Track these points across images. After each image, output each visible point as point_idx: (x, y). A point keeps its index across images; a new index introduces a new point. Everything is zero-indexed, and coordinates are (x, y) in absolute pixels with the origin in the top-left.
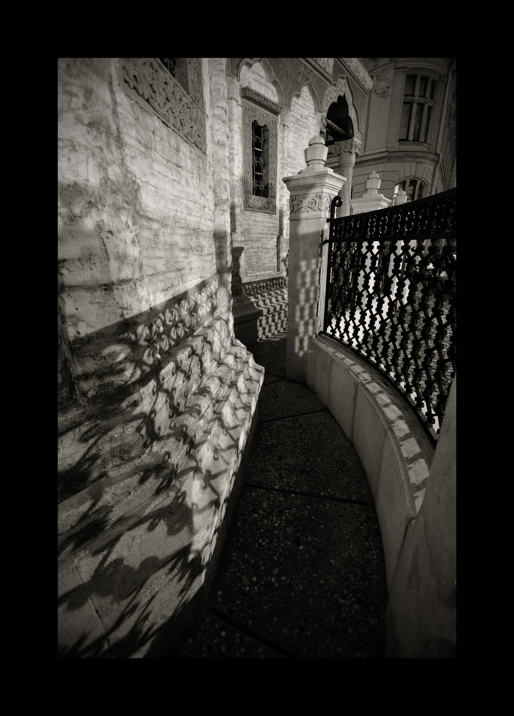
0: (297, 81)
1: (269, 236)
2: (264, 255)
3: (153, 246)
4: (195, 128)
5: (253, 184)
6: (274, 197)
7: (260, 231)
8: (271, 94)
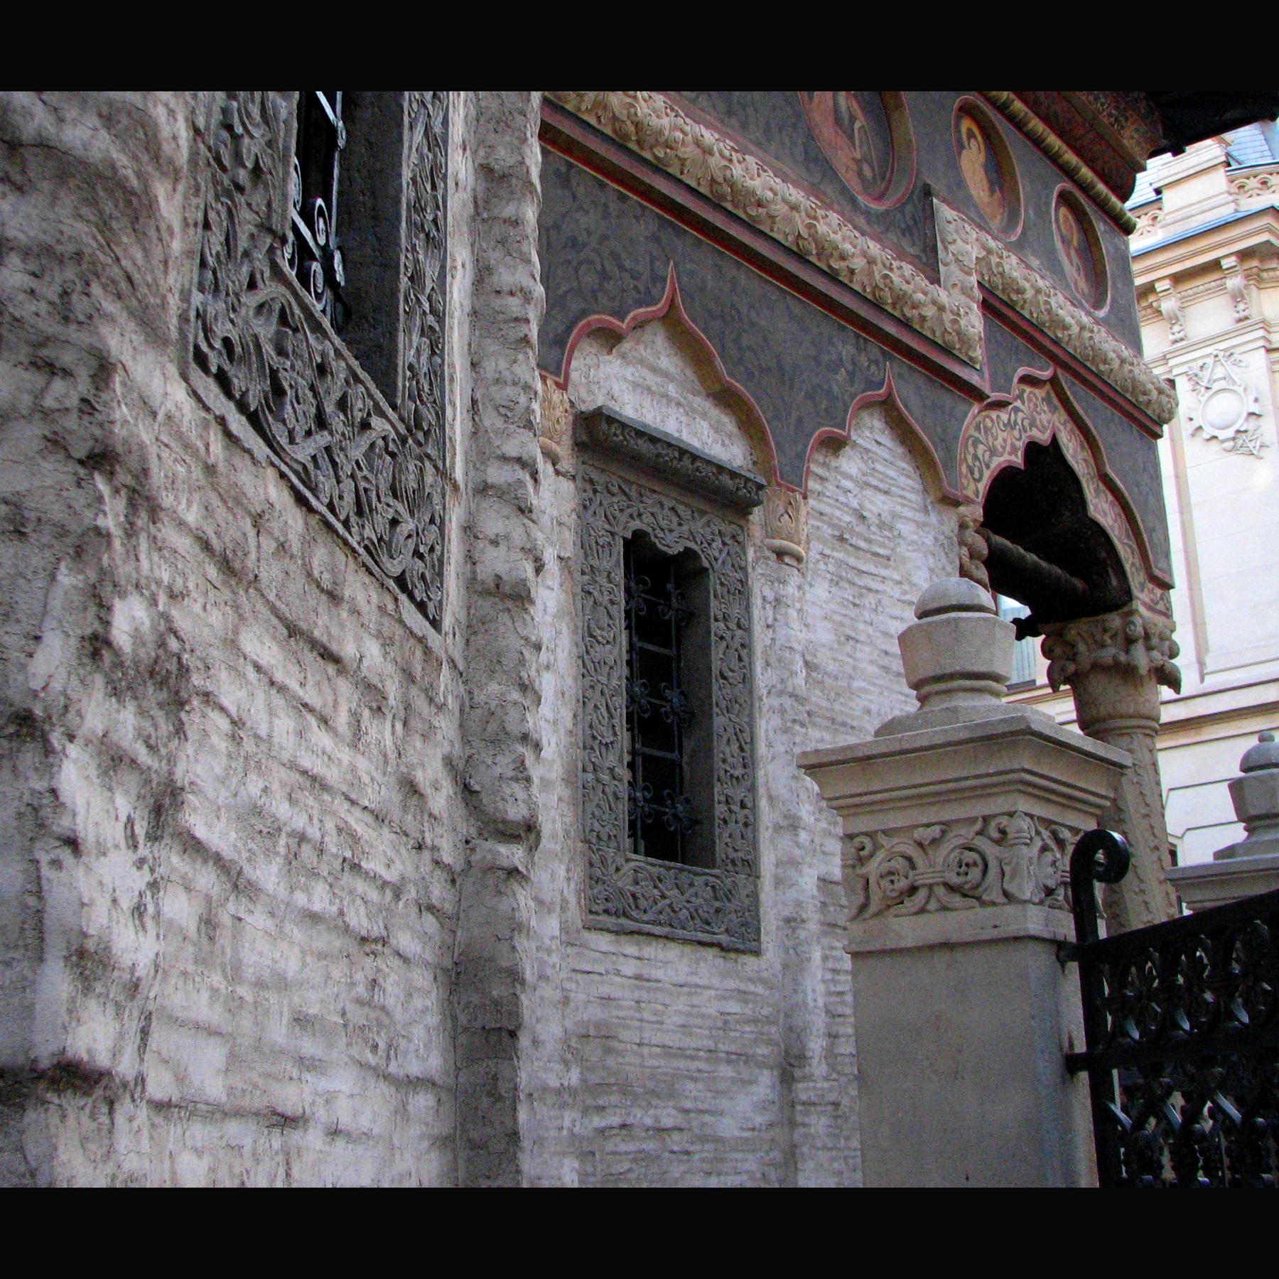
0: (828, 393)
1: (726, 1071)
3: (191, 968)
4: (408, 525)
5: (632, 799)
6: (750, 866)
7: (674, 1040)
8: (711, 437)
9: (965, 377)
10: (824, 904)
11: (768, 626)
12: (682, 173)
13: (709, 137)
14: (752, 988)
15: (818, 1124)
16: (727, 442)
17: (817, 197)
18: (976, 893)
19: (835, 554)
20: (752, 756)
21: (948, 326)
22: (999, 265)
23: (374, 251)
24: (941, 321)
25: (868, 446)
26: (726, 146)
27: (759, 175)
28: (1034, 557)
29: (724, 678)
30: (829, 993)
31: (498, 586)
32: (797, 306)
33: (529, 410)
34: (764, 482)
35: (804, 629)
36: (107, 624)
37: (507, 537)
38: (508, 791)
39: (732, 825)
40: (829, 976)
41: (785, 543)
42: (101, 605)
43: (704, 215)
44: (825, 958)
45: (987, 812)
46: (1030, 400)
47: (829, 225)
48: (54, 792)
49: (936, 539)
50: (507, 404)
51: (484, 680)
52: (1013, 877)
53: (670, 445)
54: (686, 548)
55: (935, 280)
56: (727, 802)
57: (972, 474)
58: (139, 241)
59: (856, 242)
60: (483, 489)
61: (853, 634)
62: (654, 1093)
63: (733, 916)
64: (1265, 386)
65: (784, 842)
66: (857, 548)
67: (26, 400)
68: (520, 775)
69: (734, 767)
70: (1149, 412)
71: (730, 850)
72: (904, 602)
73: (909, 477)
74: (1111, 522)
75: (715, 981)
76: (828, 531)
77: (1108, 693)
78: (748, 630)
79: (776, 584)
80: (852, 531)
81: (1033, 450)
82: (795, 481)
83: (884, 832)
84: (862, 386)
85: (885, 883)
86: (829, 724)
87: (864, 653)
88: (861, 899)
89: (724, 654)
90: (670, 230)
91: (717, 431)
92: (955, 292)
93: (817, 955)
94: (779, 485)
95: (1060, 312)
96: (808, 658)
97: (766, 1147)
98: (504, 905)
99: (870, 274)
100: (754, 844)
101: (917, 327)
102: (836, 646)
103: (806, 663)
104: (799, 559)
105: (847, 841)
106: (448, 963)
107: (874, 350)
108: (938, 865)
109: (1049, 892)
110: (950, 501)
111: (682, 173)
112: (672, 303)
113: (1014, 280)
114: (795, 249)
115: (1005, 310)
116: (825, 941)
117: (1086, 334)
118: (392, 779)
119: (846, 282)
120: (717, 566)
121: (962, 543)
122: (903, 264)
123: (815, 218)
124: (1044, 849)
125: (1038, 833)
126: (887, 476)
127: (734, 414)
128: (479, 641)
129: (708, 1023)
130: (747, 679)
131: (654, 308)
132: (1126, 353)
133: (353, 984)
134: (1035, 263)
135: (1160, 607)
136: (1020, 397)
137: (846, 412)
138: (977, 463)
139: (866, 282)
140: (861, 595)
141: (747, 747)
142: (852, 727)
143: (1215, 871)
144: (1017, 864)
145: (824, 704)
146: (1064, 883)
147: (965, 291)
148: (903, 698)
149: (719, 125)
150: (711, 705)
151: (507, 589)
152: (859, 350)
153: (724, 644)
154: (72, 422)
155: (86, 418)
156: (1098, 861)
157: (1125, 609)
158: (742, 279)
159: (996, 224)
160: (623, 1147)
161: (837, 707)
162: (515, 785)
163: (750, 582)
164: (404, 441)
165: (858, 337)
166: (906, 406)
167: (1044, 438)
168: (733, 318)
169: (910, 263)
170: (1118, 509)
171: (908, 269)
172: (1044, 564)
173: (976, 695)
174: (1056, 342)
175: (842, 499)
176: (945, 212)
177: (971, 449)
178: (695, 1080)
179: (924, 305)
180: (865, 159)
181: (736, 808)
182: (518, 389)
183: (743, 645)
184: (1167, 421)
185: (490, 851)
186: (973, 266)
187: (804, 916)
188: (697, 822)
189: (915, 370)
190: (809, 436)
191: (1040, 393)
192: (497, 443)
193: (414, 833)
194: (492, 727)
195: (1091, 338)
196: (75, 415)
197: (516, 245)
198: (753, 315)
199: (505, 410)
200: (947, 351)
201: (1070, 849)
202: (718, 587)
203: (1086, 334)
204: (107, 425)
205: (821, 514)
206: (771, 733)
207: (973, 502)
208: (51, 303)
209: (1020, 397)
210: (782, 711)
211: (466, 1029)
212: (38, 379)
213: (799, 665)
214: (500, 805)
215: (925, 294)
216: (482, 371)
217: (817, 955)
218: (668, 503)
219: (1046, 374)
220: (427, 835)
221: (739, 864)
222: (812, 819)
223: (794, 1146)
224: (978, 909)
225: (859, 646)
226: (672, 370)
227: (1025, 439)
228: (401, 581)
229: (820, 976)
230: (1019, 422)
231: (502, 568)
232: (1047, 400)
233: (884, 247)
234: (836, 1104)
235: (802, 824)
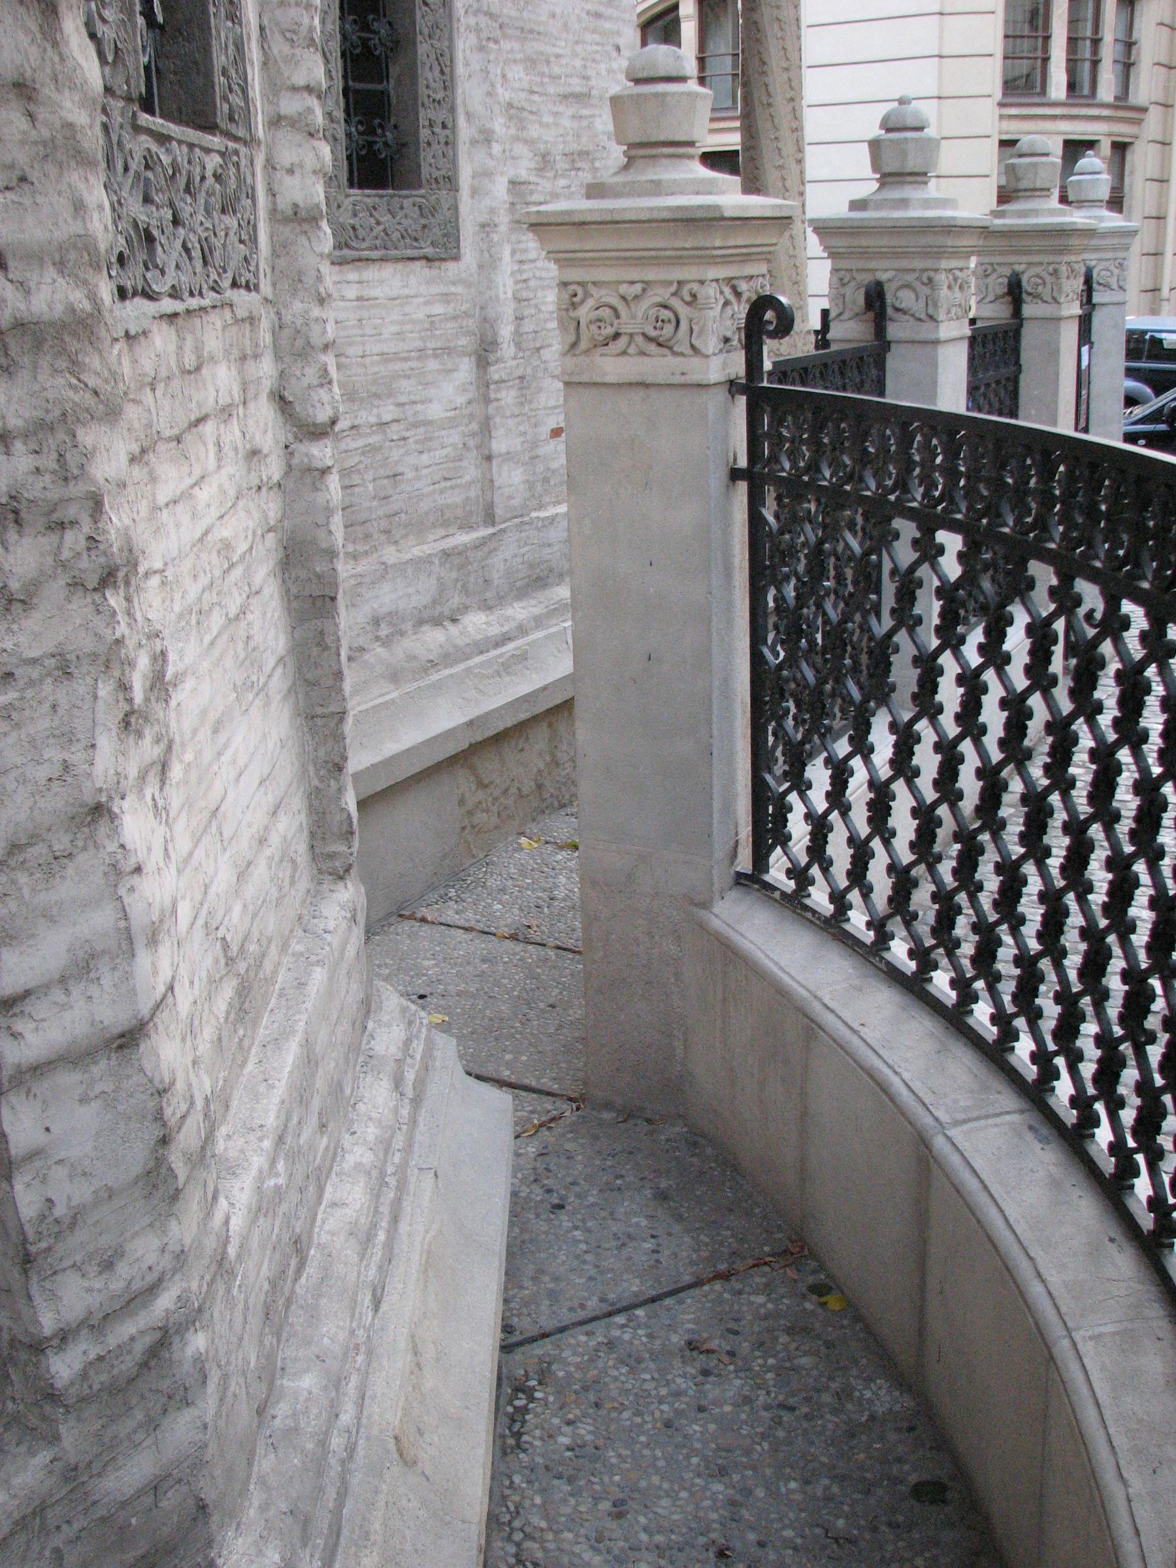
1: (433, 365)
2: (412, 460)
5: (349, 135)
6: (450, 181)
7: (389, 348)
10: (513, 204)
14: (453, 289)
15: (508, 397)
30: (516, 282)
33: (311, 29)
37: (301, 166)
38: (316, 398)
39: (435, 146)
44: (513, 252)
45: (681, 278)
48: (122, 846)
62: (376, 396)
63: (436, 230)
65: (480, 155)
67: (49, 560)
69: (435, 92)
75: (423, 289)
83: (594, 283)
85: (593, 327)
86: (518, 33)
88: (572, 338)
97: (466, 421)
98: (320, 498)
100: (454, 163)
108: (636, 319)
116: (513, 237)
128: (282, 263)
141: (447, 70)
151: (303, 214)
154: (84, 563)
155: (93, 553)
160: (353, 445)
161: (525, 14)
173: (676, 161)
178: (408, 377)
181: (438, 130)
188: (404, 145)
196: (85, 556)
208: (54, 472)
210: (478, 30)
211: (296, 597)
212: (54, 538)
214: (310, 410)
223: (488, 419)
234: (522, 378)
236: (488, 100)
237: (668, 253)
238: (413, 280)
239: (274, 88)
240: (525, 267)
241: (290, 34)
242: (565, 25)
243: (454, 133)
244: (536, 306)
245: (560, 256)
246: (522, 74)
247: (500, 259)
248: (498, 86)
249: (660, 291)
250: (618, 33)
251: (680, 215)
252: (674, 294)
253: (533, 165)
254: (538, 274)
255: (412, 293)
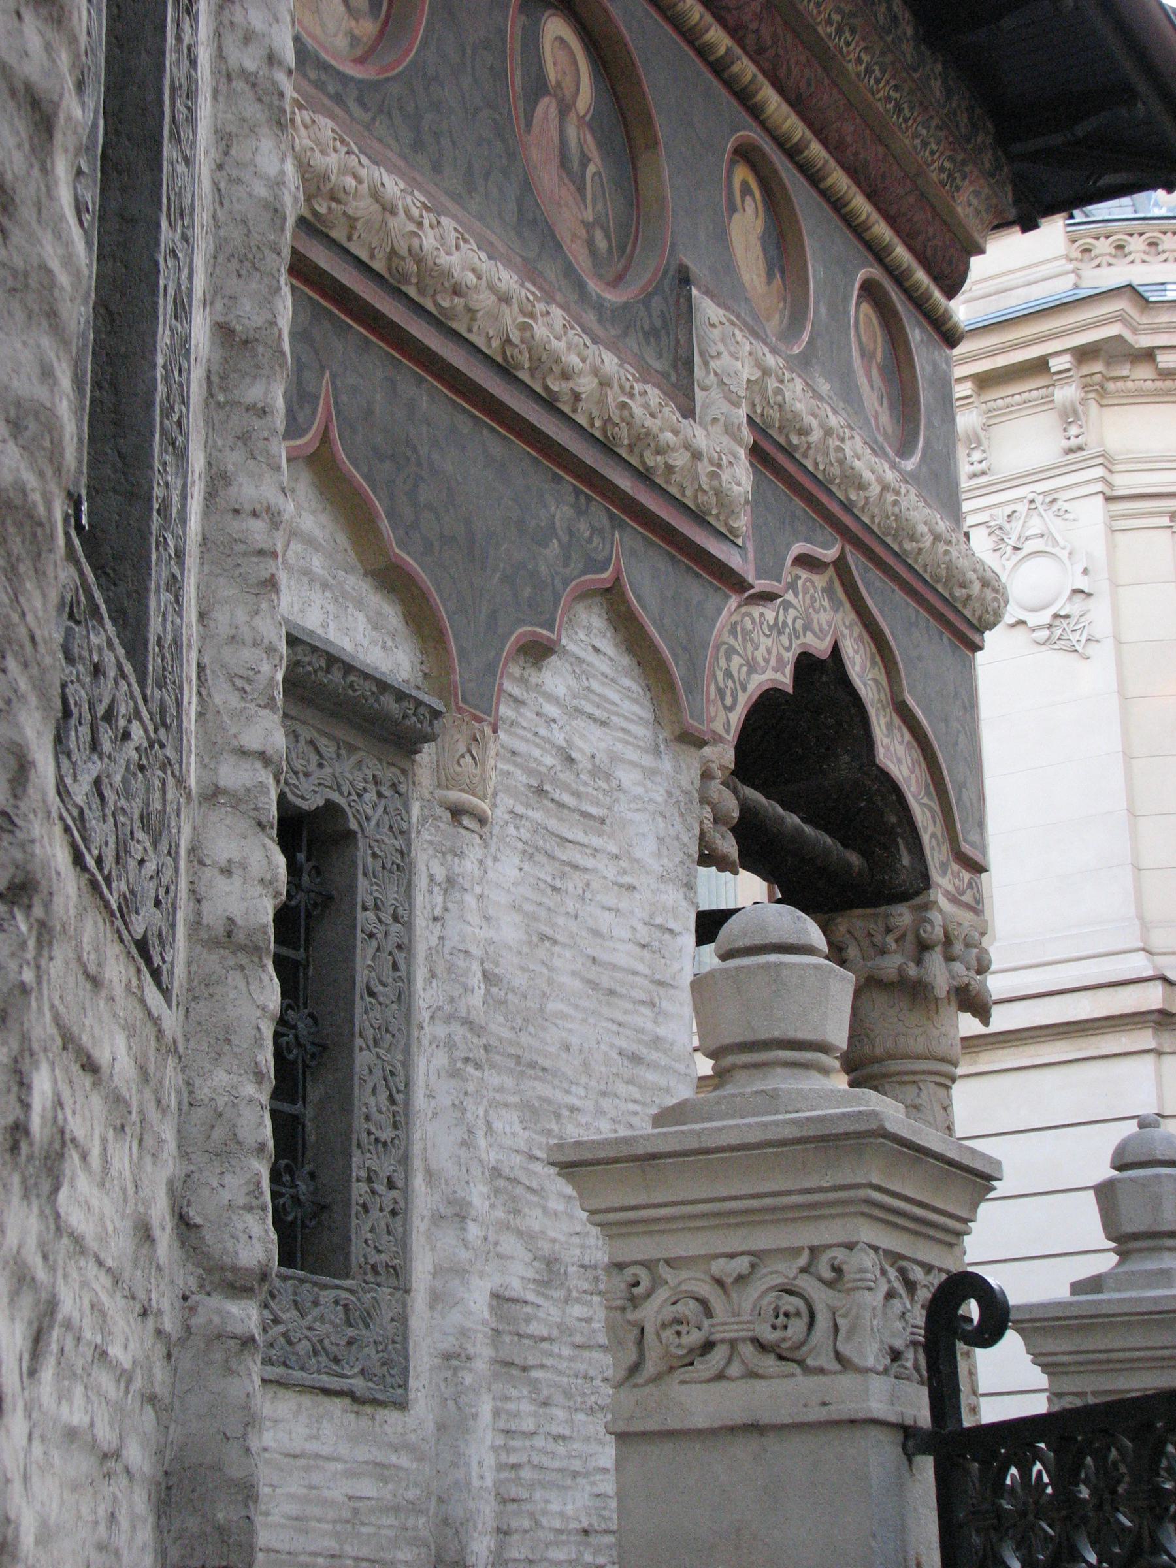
4: (151, 867)
6: (397, 1273)
8: (372, 639)
9: (721, 557)
11: (435, 919)
12: (350, 239)
13: (393, 186)
14: (394, 1459)
16: (390, 643)
17: (534, 284)
18: (797, 1355)
19: (530, 813)
20: (406, 1115)
21: (704, 481)
22: (778, 391)
23: (115, 472)
24: (696, 477)
25: (582, 654)
26: (414, 201)
27: (458, 248)
28: (797, 819)
29: (372, 994)
30: (501, 1467)
31: (229, 934)
32: (496, 445)
34: (443, 709)
35: (484, 924)
36: (26, 1106)
37: (243, 866)
39: (375, 1213)
40: (500, 1441)
41: (465, 797)
42: (21, 1084)
43: (378, 306)
44: (496, 1413)
45: (816, 1242)
46: (805, 593)
47: (550, 326)
49: (669, 794)
50: (245, 673)
51: (208, 1067)
52: (849, 1338)
53: (315, 649)
54: (327, 801)
55: (688, 412)
56: (369, 1180)
57: (722, 698)
58: (40, 587)
59: (588, 352)
60: (213, 795)
61: (548, 931)
63: (371, 1350)
64: (1099, 549)
65: (447, 1239)
66: (561, 805)
68: (255, 1203)
70: (967, 613)
71: (370, 1251)
72: (621, 886)
73: (636, 701)
74: (906, 772)
75: (344, 1450)
76: (521, 778)
77: (894, 1025)
78: (408, 925)
79: (449, 857)
80: (554, 781)
81: (806, 665)
82: (482, 708)
83: (668, 1262)
84: (581, 566)
85: (668, 1334)
86: (511, 1064)
87: (564, 960)
88: (633, 1357)
89: (373, 959)
90: (326, 323)
91: (375, 628)
92: (717, 430)
93: (486, 1409)
94: (459, 709)
95: (857, 464)
96: (487, 966)
99: (602, 401)
100: (404, 1244)
101: (660, 481)
102: (525, 949)
103: (485, 974)
104: (482, 821)
105: (615, 1272)
106: (161, 1473)
107: (599, 513)
108: (743, 1314)
109: (896, 1355)
110: (691, 739)
111: (350, 239)
112: (325, 439)
113: (796, 415)
114: (500, 360)
115: (781, 458)
117: (890, 497)
118: (128, 1223)
119: (567, 409)
120: (370, 828)
121: (704, 800)
122: (648, 388)
123: (532, 316)
124: (890, 1295)
125: (884, 1272)
126: (607, 700)
127: (403, 602)
128: (201, 1009)
129: (331, 1514)
130: (404, 997)
131: (299, 442)
132: (942, 526)
133: (97, 1523)
134: (824, 387)
135: (967, 898)
136: (792, 586)
137: (557, 599)
138: (730, 684)
139: (595, 413)
140: (564, 874)
141: (399, 1098)
142: (544, 1069)
143: (1075, 1312)
144: (857, 1317)
145: (507, 1034)
146: (914, 1344)
147: (730, 430)
148: (615, 1028)
149: (400, 163)
150: (353, 1035)
152: (581, 512)
153: (374, 943)
156: (961, 1313)
157: (917, 901)
158: (424, 402)
159: (774, 325)
162: (249, 1217)
163: (413, 854)
164: (151, 746)
165: (577, 492)
166: (638, 597)
167: (821, 647)
168: (408, 459)
169: (656, 385)
170: (917, 753)
171: (654, 396)
172: (808, 829)
174: (847, 507)
175: (543, 732)
176: (708, 309)
177: (723, 663)
179: (673, 450)
180: (597, 221)
181: (381, 1188)
182: (259, 652)
183: (399, 947)
184: (990, 626)
185: (219, 1312)
186: (742, 393)
187: (471, 1351)
188: (324, 1207)
189: (652, 543)
190: (505, 638)
191: (820, 581)
192: (232, 731)
193: (142, 1295)
194: (218, 1134)
195: (896, 503)
197: (261, 444)
198: (436, 456)
199: (242, 682)
200: (699, 518)
201: (924, 1295)
202: (370, 860)
203: (890, 497)
204: (28, 846)
205: (514, 753)
206: (433, 1078)
207: (721, 740)
209: (792, 586)
210: (450, 1045)
213: (476, 979)
214: (229, 1244)
215: (676, 433)
216: (212, 624)
217: (486, 1409)
218: (305, 733)
219: (830, 554)
220: (154, 1295)
221: (382, 1270)
222: (487, 1204)
224: (800, 1378)
225: (557, 949)
226: (318, 533)
227: (796, 650)
228: (142, 946)
229: (488, 1443)
230: (790, 622)
231: (236, 909)
232: (829, 591)
233: (622, 361)
235: (473, 1213)
236: (462, 1152)
237: (795, 1199)
238: (327, 1429)
239: (213, 750)
240: (516, 1443)
241: (242, 682)
242: (585, 1064)
243: (406, 1199)
244: (532, 1515)
245: (612, 1217)
246: (517, 1127)
247: (475, 1416)
248: (480, 1133)
249: (781, 1266)
250: (668, 1090)
251: (812, 1132)
252: (804, 1270)
253: (531, 1274)
254: (536, 1460)
255: (326, 1450)
